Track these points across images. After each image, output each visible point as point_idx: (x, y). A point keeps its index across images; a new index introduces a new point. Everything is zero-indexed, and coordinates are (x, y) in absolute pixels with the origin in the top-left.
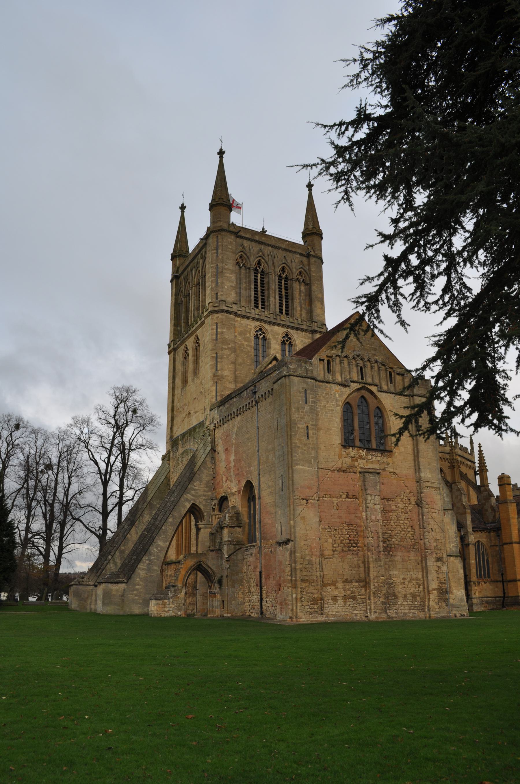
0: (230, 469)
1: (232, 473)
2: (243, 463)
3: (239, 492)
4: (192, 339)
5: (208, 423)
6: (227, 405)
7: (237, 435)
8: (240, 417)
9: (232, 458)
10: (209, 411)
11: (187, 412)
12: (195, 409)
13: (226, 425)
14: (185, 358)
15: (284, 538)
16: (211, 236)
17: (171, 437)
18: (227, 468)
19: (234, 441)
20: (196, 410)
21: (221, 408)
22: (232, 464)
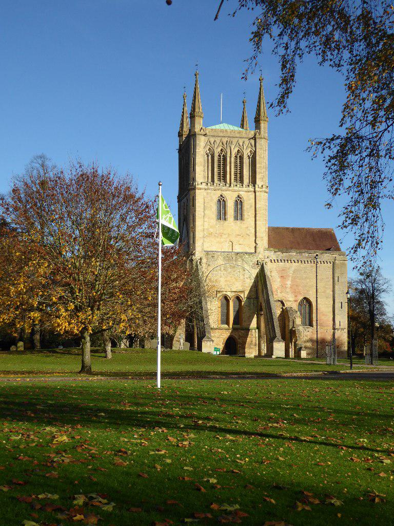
0: (286, 288)
1: (288, 290)
2: (300, 288)
3: (296, 301)
4: (236, 195)
5: (260, 256)
6: (285, 254)
7: (294, 272)
8: (297, 264)
9: (289, 283)
10: (262, 250)
11: (228, 240)
12: (239, 241)
13: (282, 264)
14: (219, 201)
15: (341, 327)
16: (263, 140)
17: (203, 249)
18: (283, 286)
19: (291, 275)
20: (241, 242)
21: (279, 253)
22: (289, 286)
